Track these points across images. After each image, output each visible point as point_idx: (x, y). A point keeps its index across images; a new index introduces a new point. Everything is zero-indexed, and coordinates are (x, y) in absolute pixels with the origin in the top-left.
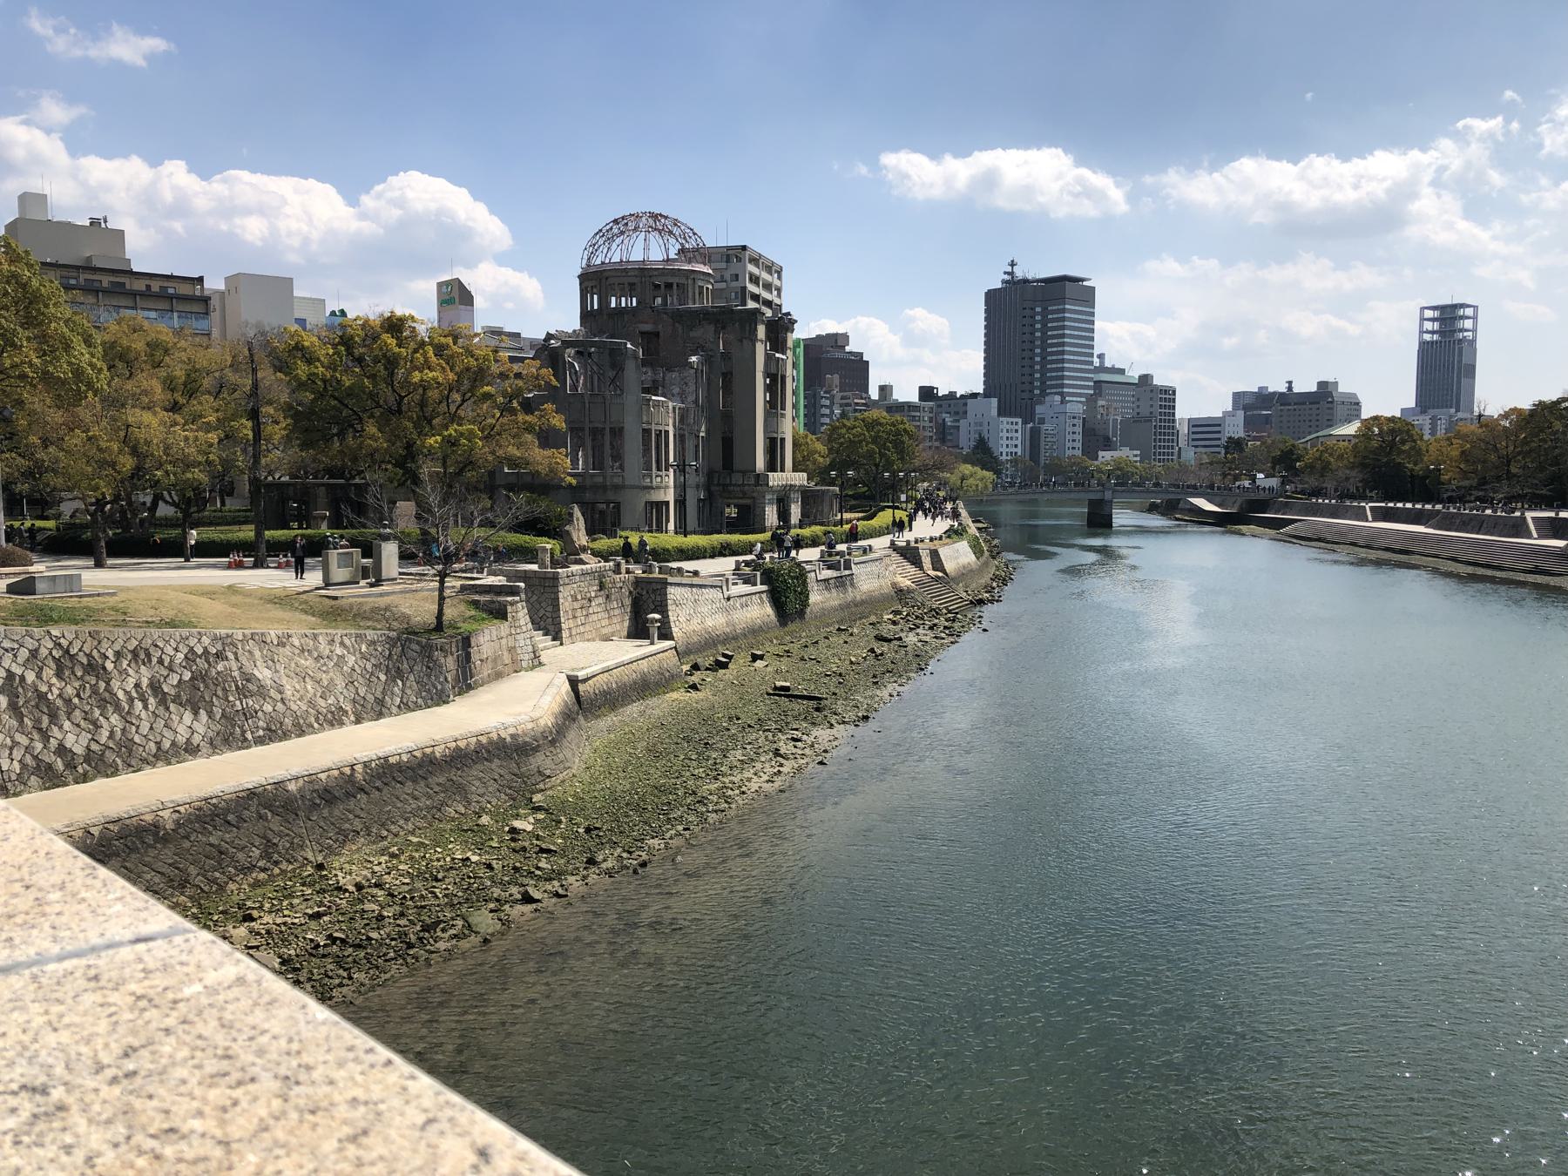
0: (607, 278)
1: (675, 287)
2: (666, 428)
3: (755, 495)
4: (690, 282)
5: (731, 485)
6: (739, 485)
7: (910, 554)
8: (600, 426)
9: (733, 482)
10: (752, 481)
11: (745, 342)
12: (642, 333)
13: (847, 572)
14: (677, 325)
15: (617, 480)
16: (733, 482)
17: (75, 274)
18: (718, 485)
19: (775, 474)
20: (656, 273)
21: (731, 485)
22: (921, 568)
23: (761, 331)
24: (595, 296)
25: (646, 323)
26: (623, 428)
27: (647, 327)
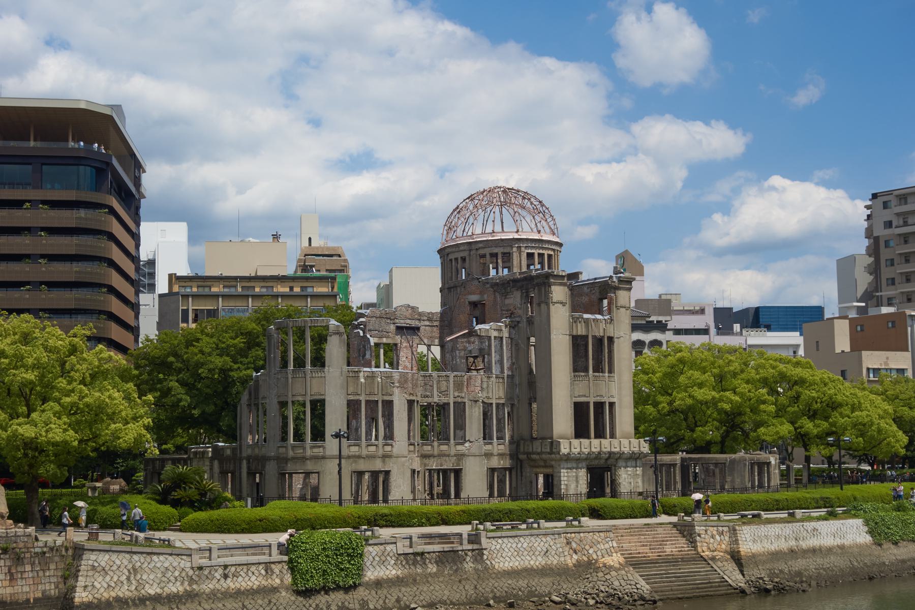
0: (448, 255)
1: (500, 256)
2: (387, 398)
3: (553, 463)
4: (515, 249)
5: (534, 453)
6: (538, 454)
7: (687, 531)
8: (300, 399)
9: (534, 450)
10: (548, 450)
11: (543, 306)
12: (474, 305)
13: (470, 547)
14: (497, 294)
15: (318, 451)
16: (534, 450)
17: (234, 283)
18: (524, 453)
19: (576, 442)
20: (481, 245)
21: (534, 453)
22: (695, 547)
23: (558, 293)
24: (463, 270)
25: (474, 294)
26: (322, 402)
27: (474, 298)
